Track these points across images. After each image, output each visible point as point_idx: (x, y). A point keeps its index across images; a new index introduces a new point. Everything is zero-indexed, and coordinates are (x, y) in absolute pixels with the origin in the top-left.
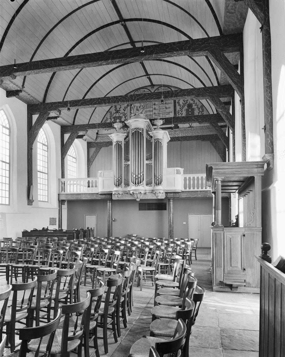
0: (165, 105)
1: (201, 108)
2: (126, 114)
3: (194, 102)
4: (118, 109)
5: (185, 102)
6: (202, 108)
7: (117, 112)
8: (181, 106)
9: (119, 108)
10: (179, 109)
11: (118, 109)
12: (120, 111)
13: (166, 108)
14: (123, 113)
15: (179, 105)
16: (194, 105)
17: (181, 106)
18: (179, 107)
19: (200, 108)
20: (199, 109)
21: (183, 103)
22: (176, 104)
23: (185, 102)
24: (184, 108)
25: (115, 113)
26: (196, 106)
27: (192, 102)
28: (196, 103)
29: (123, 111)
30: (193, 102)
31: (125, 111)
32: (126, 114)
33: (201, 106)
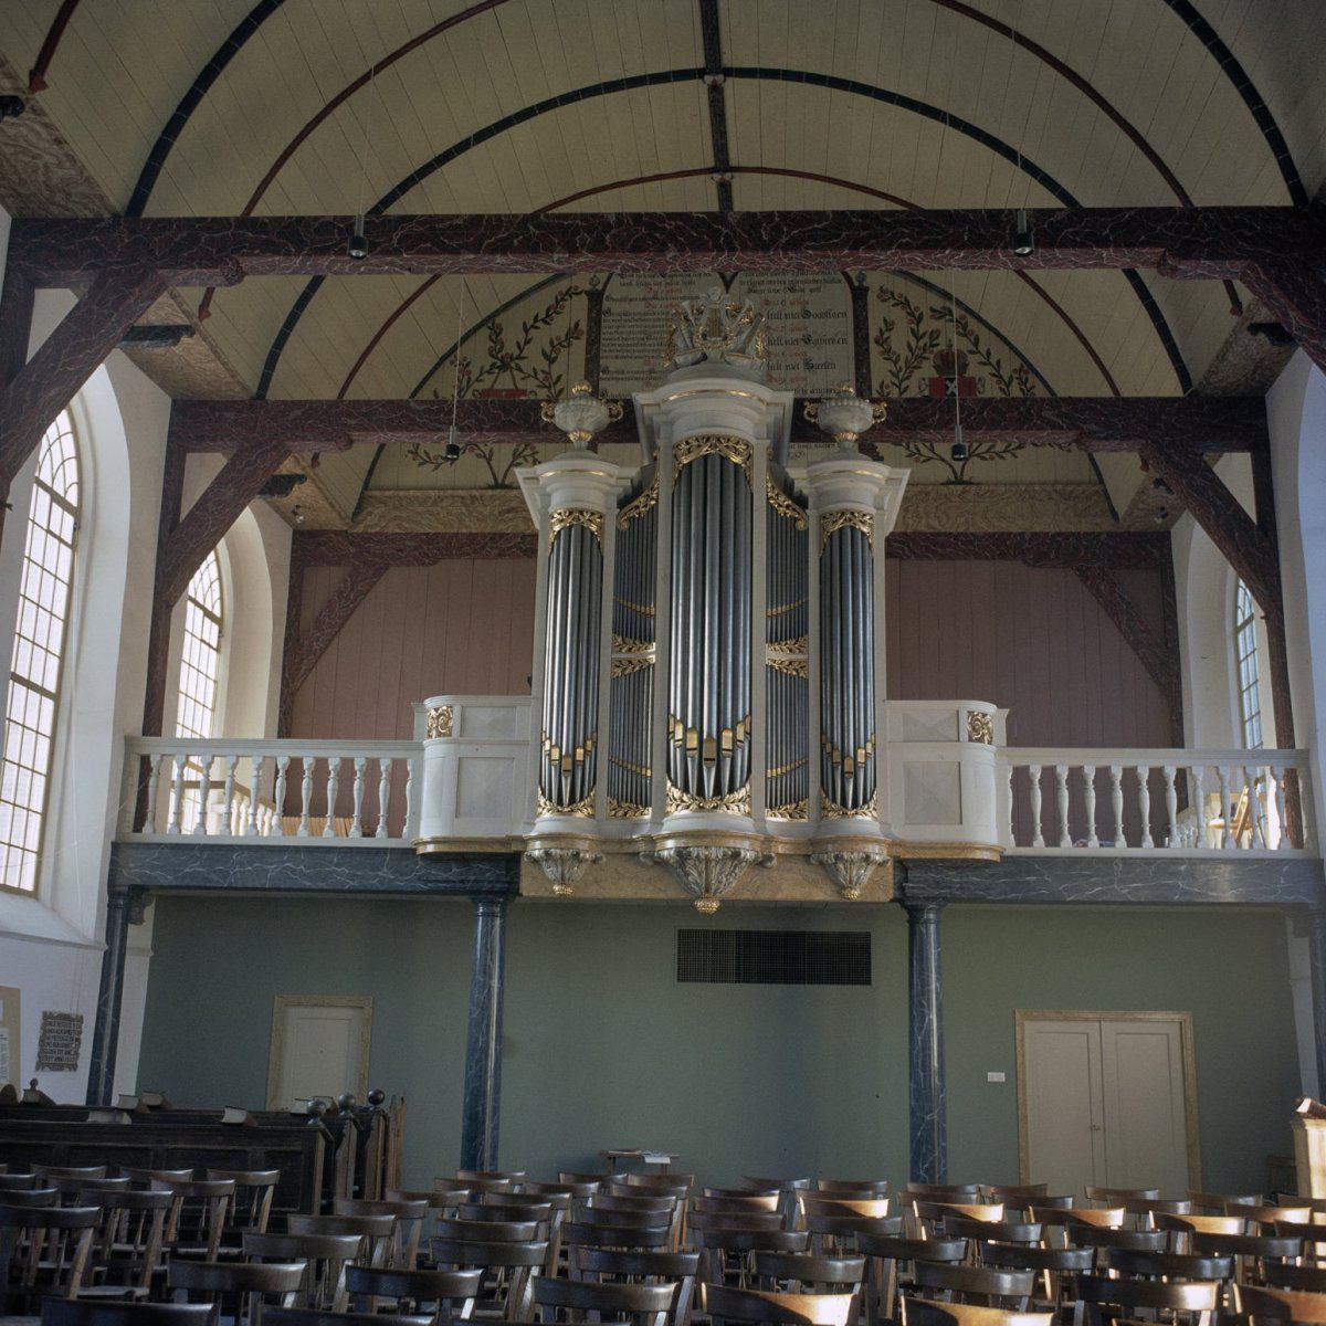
0: (802, 348)
1: (1015, 382)
2: (559, 378)
3: (976, 344)
4: (511, 349)
5: (922, 343)
6: (1023, 382)
7: (504, 367)
8: (896, 363)
9: (518, 344)
10: (889, 379)
11: (511, 349)
12: (519, 358)
13: (809, 366)
14: (541, 376)
15: (887, 353)
16: (973, 360)
17: (896, 363)
18: (889, 365)
19: (1011, 379)
20: (1008, 387)
21: (909, 346)
22: (867, 350)
23: (922, 343)
24: (917, 374)
25: (489, 372)
26: (989, 369)
27: (960, 344)
28: (989, 353)
29: (544, 365)
30: (972, 348)
31: (552, 361)
32: (559, 378)
33: (1015, 371)
